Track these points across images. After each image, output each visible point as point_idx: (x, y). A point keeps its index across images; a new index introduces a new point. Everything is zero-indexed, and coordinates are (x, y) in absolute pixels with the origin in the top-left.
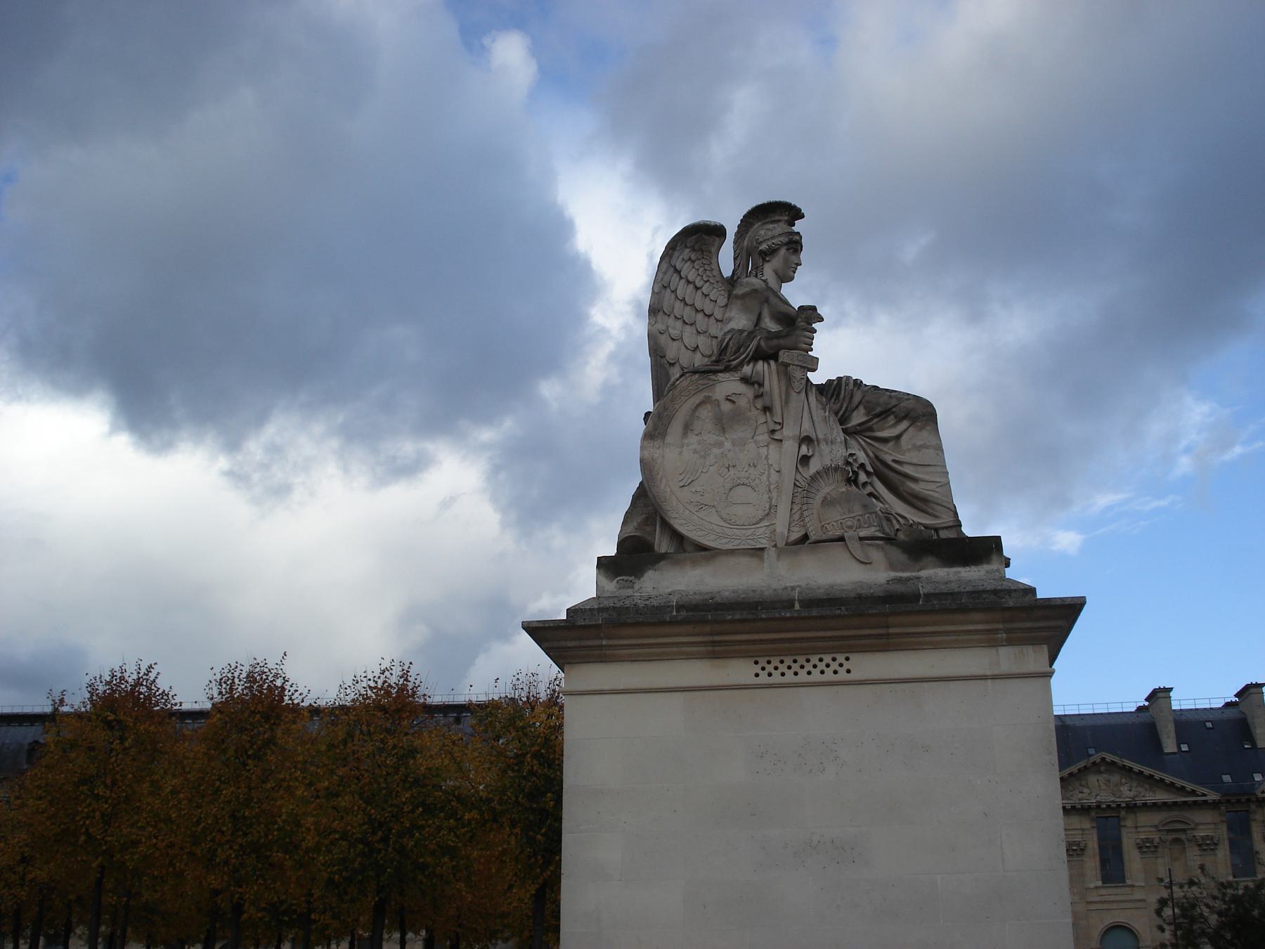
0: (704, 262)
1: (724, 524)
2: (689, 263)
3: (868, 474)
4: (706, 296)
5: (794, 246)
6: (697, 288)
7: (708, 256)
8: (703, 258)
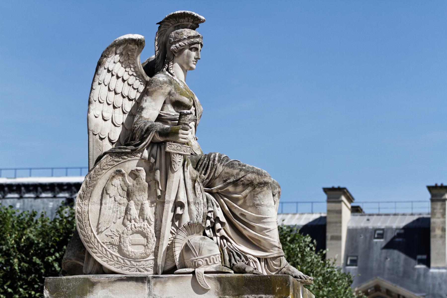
0: (130, 62)
3: (222, 224)
4: (130, 85)
6: (124, 81)
7: (132, 58)
8: (129, 59)
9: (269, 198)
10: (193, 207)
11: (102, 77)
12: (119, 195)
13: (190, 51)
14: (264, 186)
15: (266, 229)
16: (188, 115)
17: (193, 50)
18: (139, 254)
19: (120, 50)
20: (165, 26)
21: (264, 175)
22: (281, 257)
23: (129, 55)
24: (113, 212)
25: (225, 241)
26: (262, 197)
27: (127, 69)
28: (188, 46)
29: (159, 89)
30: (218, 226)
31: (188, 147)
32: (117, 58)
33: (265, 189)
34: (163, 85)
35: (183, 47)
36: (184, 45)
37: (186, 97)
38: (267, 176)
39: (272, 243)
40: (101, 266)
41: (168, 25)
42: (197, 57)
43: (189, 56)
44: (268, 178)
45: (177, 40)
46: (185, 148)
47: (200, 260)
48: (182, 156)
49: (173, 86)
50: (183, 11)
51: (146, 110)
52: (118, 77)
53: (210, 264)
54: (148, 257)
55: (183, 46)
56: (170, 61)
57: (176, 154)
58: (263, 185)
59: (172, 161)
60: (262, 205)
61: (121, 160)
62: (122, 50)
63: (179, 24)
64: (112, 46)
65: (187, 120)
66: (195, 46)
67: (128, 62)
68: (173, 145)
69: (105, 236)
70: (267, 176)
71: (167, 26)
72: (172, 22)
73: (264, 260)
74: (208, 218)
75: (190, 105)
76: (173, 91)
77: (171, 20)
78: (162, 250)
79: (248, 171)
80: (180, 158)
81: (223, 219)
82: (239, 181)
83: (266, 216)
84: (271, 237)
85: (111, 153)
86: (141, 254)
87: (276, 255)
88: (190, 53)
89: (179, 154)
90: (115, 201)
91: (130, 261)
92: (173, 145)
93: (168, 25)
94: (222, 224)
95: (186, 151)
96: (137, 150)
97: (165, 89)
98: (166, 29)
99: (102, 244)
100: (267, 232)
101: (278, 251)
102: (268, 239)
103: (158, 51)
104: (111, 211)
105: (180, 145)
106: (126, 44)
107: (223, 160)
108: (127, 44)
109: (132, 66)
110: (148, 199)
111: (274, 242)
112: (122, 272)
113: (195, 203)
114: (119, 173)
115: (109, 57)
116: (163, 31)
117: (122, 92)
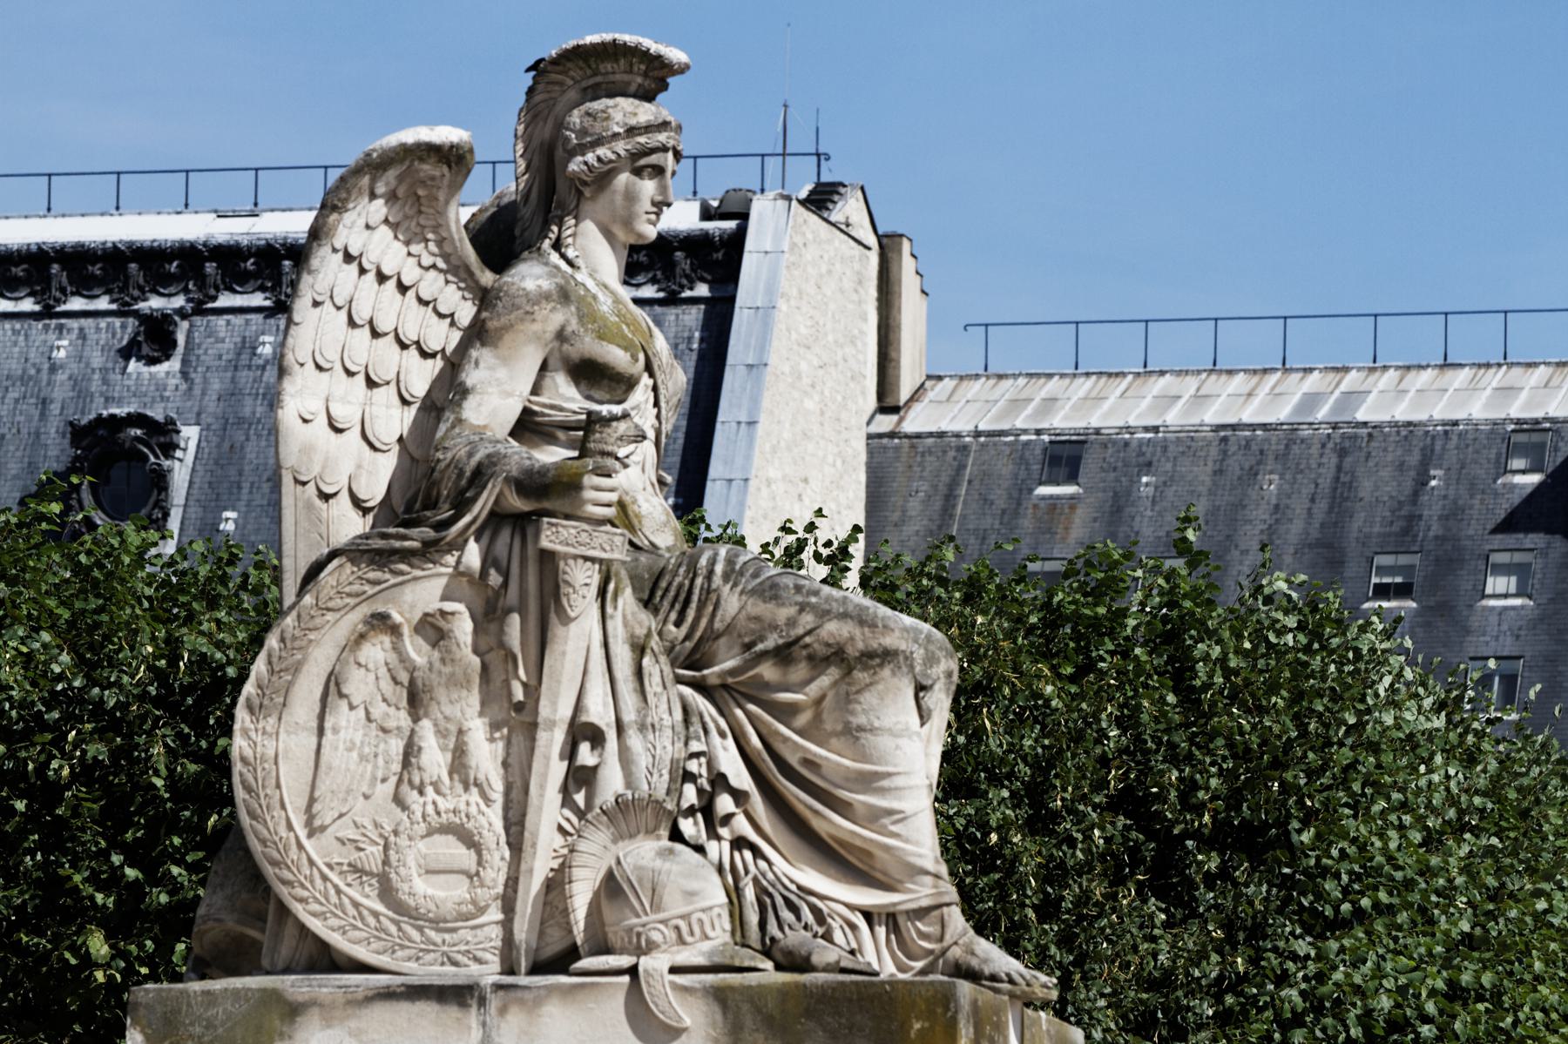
0: (422, 222)
3: (739, 796)
4: (426, 303)
6: (403, 289)
7: (429, 207)
8: (420, 212)
10: (635, 741)
12: (380, 698)
13: (636, 179)
14: (881, 665)
15: (890, 812)
16: (614, 424)
17: (645, 173)
18: (450, 905)
19: (387, 184)
20: (550, 87)
23: (419, 198)
24: (363, 758)
25: (748, 855)
26: (875, 701)
27: (415, 248)
28: (629, 162)
29: (522, 320)
30: (725, 803)
31: (616, 534)
32: (377, 211)
33: (886, 672)
34: (536, 308)
36: (613, 157)
37: (619, 346)
39: (913, 860)
40: (324, 946)
41: (561, 84)
42: (659, 198)
43: (631, 197)
44: (897, 633)
45: (589, 139)
46: (605, 537)
47: (654, 929)
48: (597, 566)
49: (573, 309)
50: (608, 37)
51: (478, 397)
52: (382, 278)
53: (689, 939)
54: (483, 913)
55: (611, 161)
56: (568, 215)
57: (575, 557)
58: (878, 661)
59: (562, 585)
60: (877, 729)
61: (387, 576)
62: (393, 183)
63: (599, 79)
64: (357, 171)
65: (612, 440)
66: (654, 159)
67: (418, 224)
68: (563, 526)
69: (335, 842)
71: (557, 88)
72: (572, 73)
73: (884, 918)
74: (689, 777)
75: (632, 375)
76: (574, 325)
77: (569, 65)
78: (527, 892)
79: (828, 612)
80: (589, 573)
81: (740, 776)
82: (796, 648)
83: (890, 769)
84: (907, 841)
85: (355, 552)
86: (459, 904)
87: (925, 903)
88: (634, 184)
89: (586, 559)
90: (369, 719)
91: (420, 929)
92: (563, 526)
93: (561, 84)
94: (739, 796)
95: (608, 548)
97: (545, 320)
98: (553, 95)
99: (326, 870)
100: (895, 822)
102: (898, 849)
103: (526, 177)
104: (355, 755)
105: (585, 526)
106: (407, 163)
107: (741, 573)
108: (412, 161)
109: (430, 236)
110: (481, 714)
111: (920, 856)
112: (393, 968)
113: (642, 728)
114: (380, 622)
115: (347, 211)
116: (543, 105)
117: (396, 329)
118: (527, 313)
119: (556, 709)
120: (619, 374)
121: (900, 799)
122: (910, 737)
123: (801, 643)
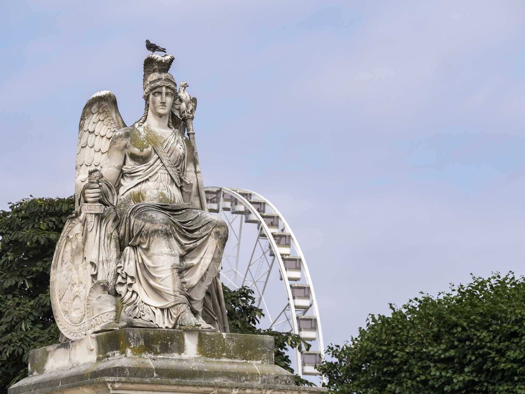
0: (110, 119)
1: (72, 324)
2: (100, 122)
5: (157, 90)
9: (159, 246)
11: (83, 140)
14: (154, 235)
16: (93, 174)
17: (156, 95)
21: (155, 223)
22: (178, 305)
24: (67, 279)
26: (154, 246)
33: (156, 236)
35: (148, 94)
38: (157, 224)
44: (158, 224)
48: (94, 215)
49: (130, 139)
65: (93, 178)
66: (157, 90)
70: (157, 224)
74: (118, 274)
75: (142, 156)
79: (146, 220)
80: (92, 218)
82: (141, 232)
84: (165, 286)
89: (91, 214)
96: (78, 214)
97: (119, 143)
101: (175, 299)
104: (65, 278)
115: (85, 119)
118: (115, 142)
119: (88, 260)
120: (137, 156)
121: (161, 274)
122: (162, 255)
123: (142, 231)
